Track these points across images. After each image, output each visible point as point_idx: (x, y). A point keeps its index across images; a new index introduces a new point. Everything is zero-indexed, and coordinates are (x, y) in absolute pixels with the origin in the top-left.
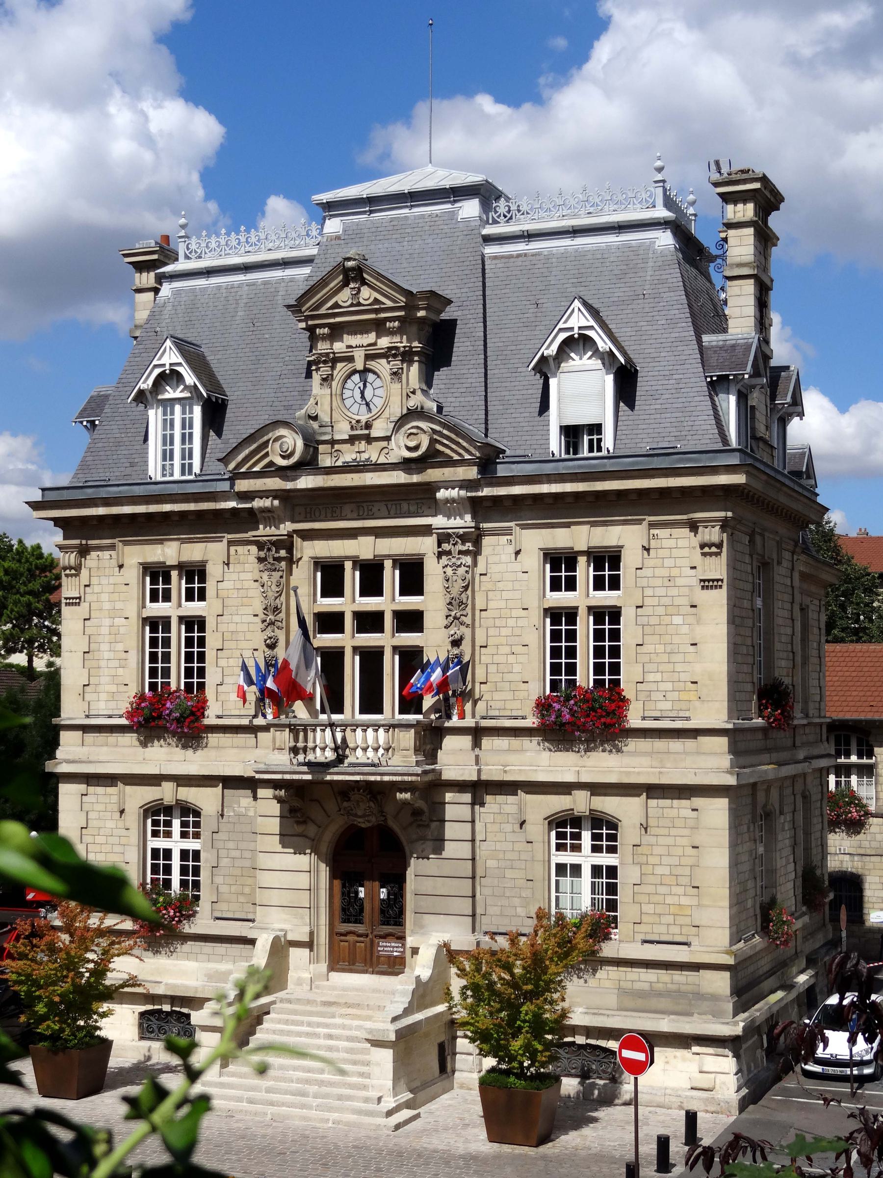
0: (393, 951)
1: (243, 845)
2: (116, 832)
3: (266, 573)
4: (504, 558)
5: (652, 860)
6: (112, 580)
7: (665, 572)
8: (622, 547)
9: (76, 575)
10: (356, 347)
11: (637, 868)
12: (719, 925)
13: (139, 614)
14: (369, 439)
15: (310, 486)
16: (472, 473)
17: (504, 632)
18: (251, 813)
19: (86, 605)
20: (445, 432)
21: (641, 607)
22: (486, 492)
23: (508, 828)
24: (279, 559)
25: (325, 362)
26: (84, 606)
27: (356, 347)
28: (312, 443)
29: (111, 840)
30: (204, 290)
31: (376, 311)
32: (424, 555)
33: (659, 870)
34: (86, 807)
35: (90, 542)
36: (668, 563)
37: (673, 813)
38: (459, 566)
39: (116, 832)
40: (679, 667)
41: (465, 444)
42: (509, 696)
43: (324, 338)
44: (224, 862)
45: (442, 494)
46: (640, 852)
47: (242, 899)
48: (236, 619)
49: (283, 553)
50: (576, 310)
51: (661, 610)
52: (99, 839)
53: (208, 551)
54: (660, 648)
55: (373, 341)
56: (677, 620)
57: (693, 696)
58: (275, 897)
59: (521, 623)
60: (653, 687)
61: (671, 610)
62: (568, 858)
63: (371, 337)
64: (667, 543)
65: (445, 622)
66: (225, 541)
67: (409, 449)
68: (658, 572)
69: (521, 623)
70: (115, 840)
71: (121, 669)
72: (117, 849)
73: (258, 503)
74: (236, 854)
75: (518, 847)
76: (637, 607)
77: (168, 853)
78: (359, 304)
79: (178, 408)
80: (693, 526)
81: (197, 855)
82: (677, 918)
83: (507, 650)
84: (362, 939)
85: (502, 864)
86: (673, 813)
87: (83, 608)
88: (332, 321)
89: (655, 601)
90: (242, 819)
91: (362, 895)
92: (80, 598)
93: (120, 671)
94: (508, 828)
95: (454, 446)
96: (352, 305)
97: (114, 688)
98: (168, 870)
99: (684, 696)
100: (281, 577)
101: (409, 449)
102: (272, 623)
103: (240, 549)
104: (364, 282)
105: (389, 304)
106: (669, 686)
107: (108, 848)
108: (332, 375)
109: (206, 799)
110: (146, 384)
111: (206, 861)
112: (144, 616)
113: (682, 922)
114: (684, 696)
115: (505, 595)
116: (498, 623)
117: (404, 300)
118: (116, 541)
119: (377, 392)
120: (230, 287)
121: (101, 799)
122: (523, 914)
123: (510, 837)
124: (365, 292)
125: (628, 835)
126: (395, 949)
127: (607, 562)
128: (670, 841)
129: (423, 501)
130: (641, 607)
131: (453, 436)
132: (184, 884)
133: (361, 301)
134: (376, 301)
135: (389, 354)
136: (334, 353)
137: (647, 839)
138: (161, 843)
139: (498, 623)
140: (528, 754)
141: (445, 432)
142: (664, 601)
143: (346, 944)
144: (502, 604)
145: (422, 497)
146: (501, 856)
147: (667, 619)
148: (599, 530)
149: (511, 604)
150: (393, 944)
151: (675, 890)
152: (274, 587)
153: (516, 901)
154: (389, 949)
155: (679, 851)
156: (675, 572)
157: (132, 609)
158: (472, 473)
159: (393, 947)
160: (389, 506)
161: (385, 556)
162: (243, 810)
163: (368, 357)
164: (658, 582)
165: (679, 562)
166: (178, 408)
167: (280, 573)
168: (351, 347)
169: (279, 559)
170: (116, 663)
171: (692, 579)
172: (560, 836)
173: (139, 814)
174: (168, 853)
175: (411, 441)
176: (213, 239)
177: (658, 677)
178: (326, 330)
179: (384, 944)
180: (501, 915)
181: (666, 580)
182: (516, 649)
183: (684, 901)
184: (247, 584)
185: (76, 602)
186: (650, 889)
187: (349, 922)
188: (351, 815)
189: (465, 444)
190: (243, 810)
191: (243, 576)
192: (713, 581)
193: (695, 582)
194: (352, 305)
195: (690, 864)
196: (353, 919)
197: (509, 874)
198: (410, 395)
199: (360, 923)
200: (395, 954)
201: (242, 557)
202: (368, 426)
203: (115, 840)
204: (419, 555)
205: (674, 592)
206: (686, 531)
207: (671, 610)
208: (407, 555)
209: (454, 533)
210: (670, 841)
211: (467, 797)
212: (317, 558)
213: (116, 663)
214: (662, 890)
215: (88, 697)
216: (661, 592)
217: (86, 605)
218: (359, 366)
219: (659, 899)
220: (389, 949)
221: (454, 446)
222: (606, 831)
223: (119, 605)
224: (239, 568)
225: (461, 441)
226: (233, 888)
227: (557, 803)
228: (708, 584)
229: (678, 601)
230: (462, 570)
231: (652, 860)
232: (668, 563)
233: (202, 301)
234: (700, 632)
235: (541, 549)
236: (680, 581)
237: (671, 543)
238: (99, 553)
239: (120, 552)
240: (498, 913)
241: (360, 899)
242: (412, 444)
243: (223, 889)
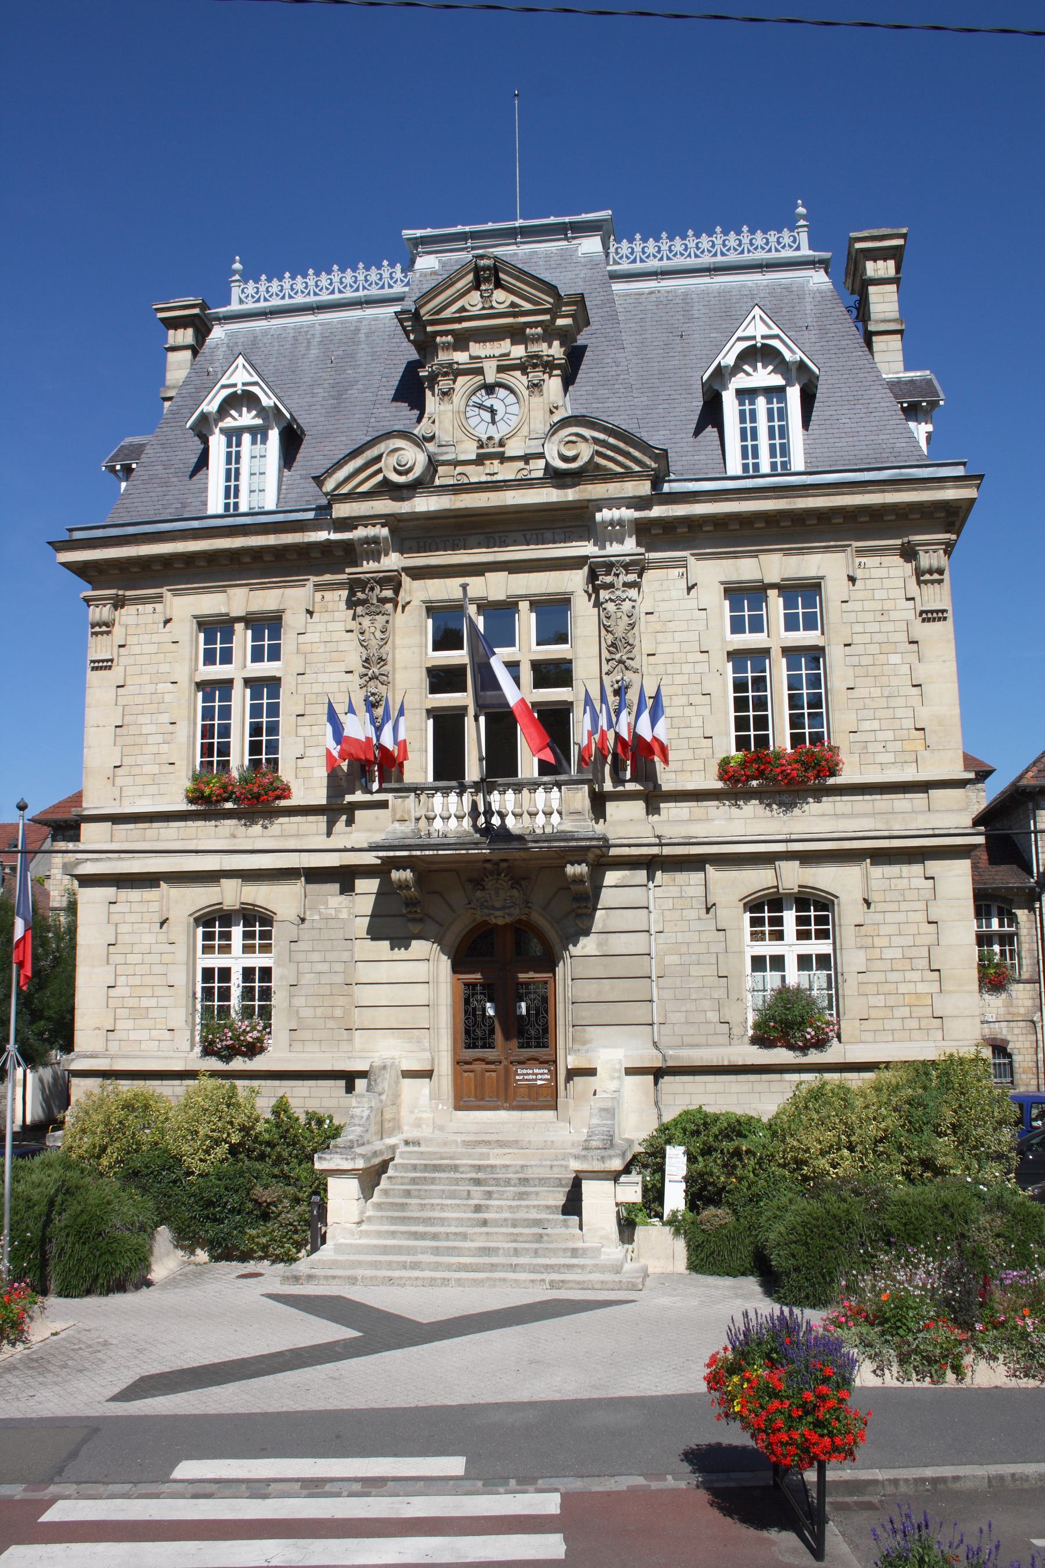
0: (536, 1080)
1: (332, 956)
2: (156, 948)
3: (368, 618)
4: (674, 594)
5: (878, 942)
6: (155, 638)
7: (877, 606)
8: (822, 578)
9: (108, 633)
10: (486, 357)
11: (862, 953)
12: (967, 1013)
13: (191, 680)
14: (503, 458)
15: (432, 508)
16: (644, 488)
17: (678, 679)
18: (344, 915)
19: (121, 669)
20: (611, 440)
21: (849, 645)
22: (657, 511)
23: (692, 914)
24: (383, 601)
25: (446, 374)
26: (117, 672)
27: (486, 357)
28: (433, 464)
29: (148, 958)
30: (265, 333)
31: (515, 315)
32: (572, 593)
33: (888, 954)
34: (115, 918)
35: (128, 593)
36: (878, 594)
37: (903, 883)
38: (624, 600)
39: (156, 948)
40: (899, 713)
41: (637, 454)
42: (689, 755)
43: (446, 347)
44: (307, 979)
45: (604, 515)
46: (863, 933)
47: (331, 1024)
48: (323, 677)
49: (388, 593)
50: (757, 318)
51: (874, 649)
52: (131, 958)
53: (288, 598)
54: (876, 692)
55: (507, 351)
56: (895, 659)
57: (919, 746)
58: (382, 1018)
59: (699, 668)
60: (871, 737)
61: (885, 648)
62: (768, 948)
63: (505, 346)
64: (875, 573)
65: (606, 668)
66: (310, 585)
67: (565, 459)
68: (868, 605)
69: (699, 668)
70: (156, 958)
71: (166, 746)
72: (158, 969)
73: (360, 533)
74: (324, 967)
75: (704, 937)
76: (846, 645)
77: (225, 974)
78: (492, 307)
79: (246, 438)
80: (909, 553)
81: (266, 973)
82: (914, 1009)
83: (683, 700)
84: (492, 1067)
85: (686, 959)
86: (903, 883)
87: (115, 675)
88: (456, 326)
89: (867, 638)
90: (332, 924)
91: (491, 1012)
92: (112, 660)
93: (165, 748)
94: (692, 914)
95: (620, 458)
96: (484, 308)
97: (155, 769)
98: (225, 994)
99: (908, 746)
100: (387, 622)
101: (565, 459)
102: (374, 677)
103: (328, 595)
104: (498, 284)
105: (527, 306)
106: (889, 735)
107: (145, 969)
108: (453, 389)
109: (281, 900)
110: (211, 405)
111: (282, 978)
112: (198, 680)
113: (920, 1015)
114: (908, 746)
115: (678, 637)
116: (670, 669)
117: (551, 300)
118: (164, 590)
119: (510, 409)
120: (298, 329)
121: (135, 907)
122: (716, 1019)
123: (696, 926)
124: (499, 295)
125: (848, 911)
126: (539, 1077)
127: (804, 592)
128: (900, 917)
129: (573, 530)
130: (849, 645)
131: (622, 445)
132: (247, 1012)
133: (494, 304)
134: (513, 305)
136: (457, 363)
137: (872, 917)
138: (216, 961)
139: (670, 669)
140: (717, 822)
141: (611, 440)
142: (878, 638)
143: (471, 1074)
144: (675, 648)
145: (576, 521)
146: (684, 949)
147: (882, 659)
148: (793, 560)
149: (685, 647)
150: (536, 1071)
151: (910, 975)
152: (378, 635)
153: (706, 1004)
154: (531, 1077)
155: (913, 929)
156: (888, 605)
157: (182, 673)
158: (644, 488)
159: (536, 1074)
160: (528, 537)
161: (520, 596)
162: (333, 912)
163: (501, 369)
164: (869, 616)
165: (893, 594)
166: (246, 438)
167: (385, 617)
168: (479, 358)
169: (383, 601)
170: (159, 738)
171: (907, 612)
172: (755, 922)
173: (188, 924)
174: (225, 974)
175: (569, 450)
176: (275, 283)
177: (876, 725)
178: (450, 338)
179: (525, 1071)
180: (687, 1023)
181: (878, 614)
182: (692, 699)
183: (921, 988)
184: (336, 637)
185: (104, 665)
186: (879, 977)
187: (475, 1047)
188: (487, 907)
189: (637, 454)
190: (333, 912)
191: (331, 627)
192: (937, 611)
193: (911, 615)
194: (484, 308)
195: (927, 943)
196: (480, 1043)
197: (695, 971)
198: (554, 410)
199: (490, 1047)
200: (539, 1082)
201: (330, 605)
202: (501, 444)
203: (156, 958)
204: (565, 593)
205: (888, 627)
206: (898, 560)
207: (885, 648)
208: (549, 594)
209: (618, 562)
210: (900, 917)
211: (641, 875)
212: (431, 602)
213: (159, 738)
214: (893, 977)
215: (119, 781)
216: (874, 627)
217: (121, 669)
218: (491, 377)
219: (891, 987)
220: (531, 1077)
221: (620, 458)
222: (816, 910)
223: (164, 668)
224: (327, 617)
225: (631, 450)
226: (319, 1012)
228: (930, 616)
229: (894, 637)
230: (627, 606)
231: (878, 942)
232: (878, 594)
233: (265, 341)
234: (922, 673)
235: (722, 583)
236: (894, 615)
237: (882, 573)
238: (139, 606)
239: (168, 604)
240: (683, 1020)
241: (490, 1017)
242: (570, 453)
243: (305, 1013)
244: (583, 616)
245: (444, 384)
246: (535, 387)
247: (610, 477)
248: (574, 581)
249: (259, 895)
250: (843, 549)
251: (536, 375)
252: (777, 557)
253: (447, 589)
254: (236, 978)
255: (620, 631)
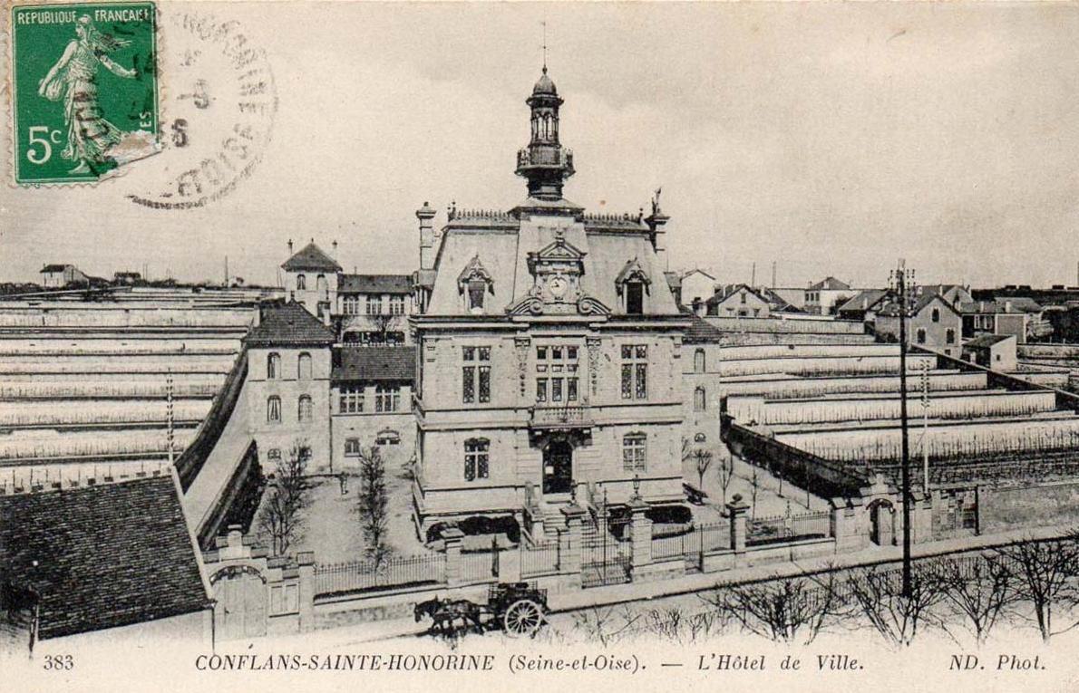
53: (493, 341)
63: (564, 266)
135: (570, 273)
171: (671, 355)
185: (433, 360)
227: (627, 429)
244: (583, 352)
245: (544, 277)
246: (572, 281)
247: (596, 314)
248: (581, 341)
249: (486, 435)
250: (654, 336)
251: (573, 277)
252: (637, 337)
253: (543, 342)
254: (477, 458)
255: (595, 358)
